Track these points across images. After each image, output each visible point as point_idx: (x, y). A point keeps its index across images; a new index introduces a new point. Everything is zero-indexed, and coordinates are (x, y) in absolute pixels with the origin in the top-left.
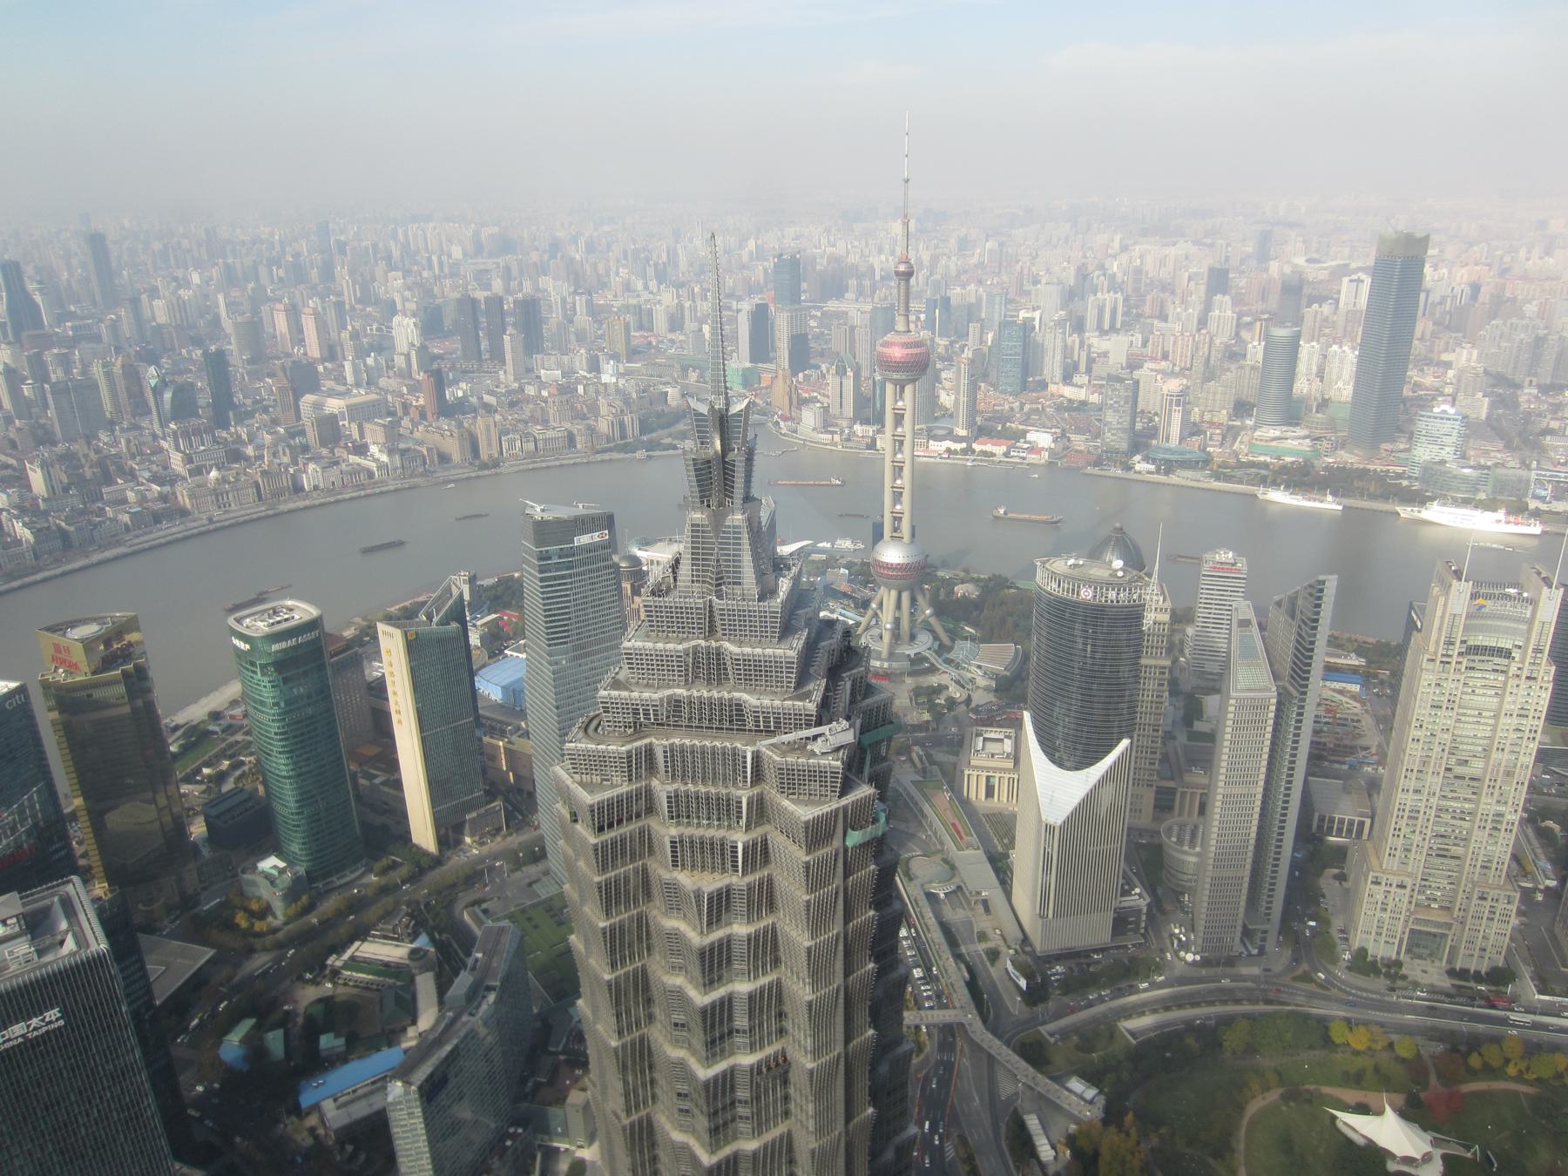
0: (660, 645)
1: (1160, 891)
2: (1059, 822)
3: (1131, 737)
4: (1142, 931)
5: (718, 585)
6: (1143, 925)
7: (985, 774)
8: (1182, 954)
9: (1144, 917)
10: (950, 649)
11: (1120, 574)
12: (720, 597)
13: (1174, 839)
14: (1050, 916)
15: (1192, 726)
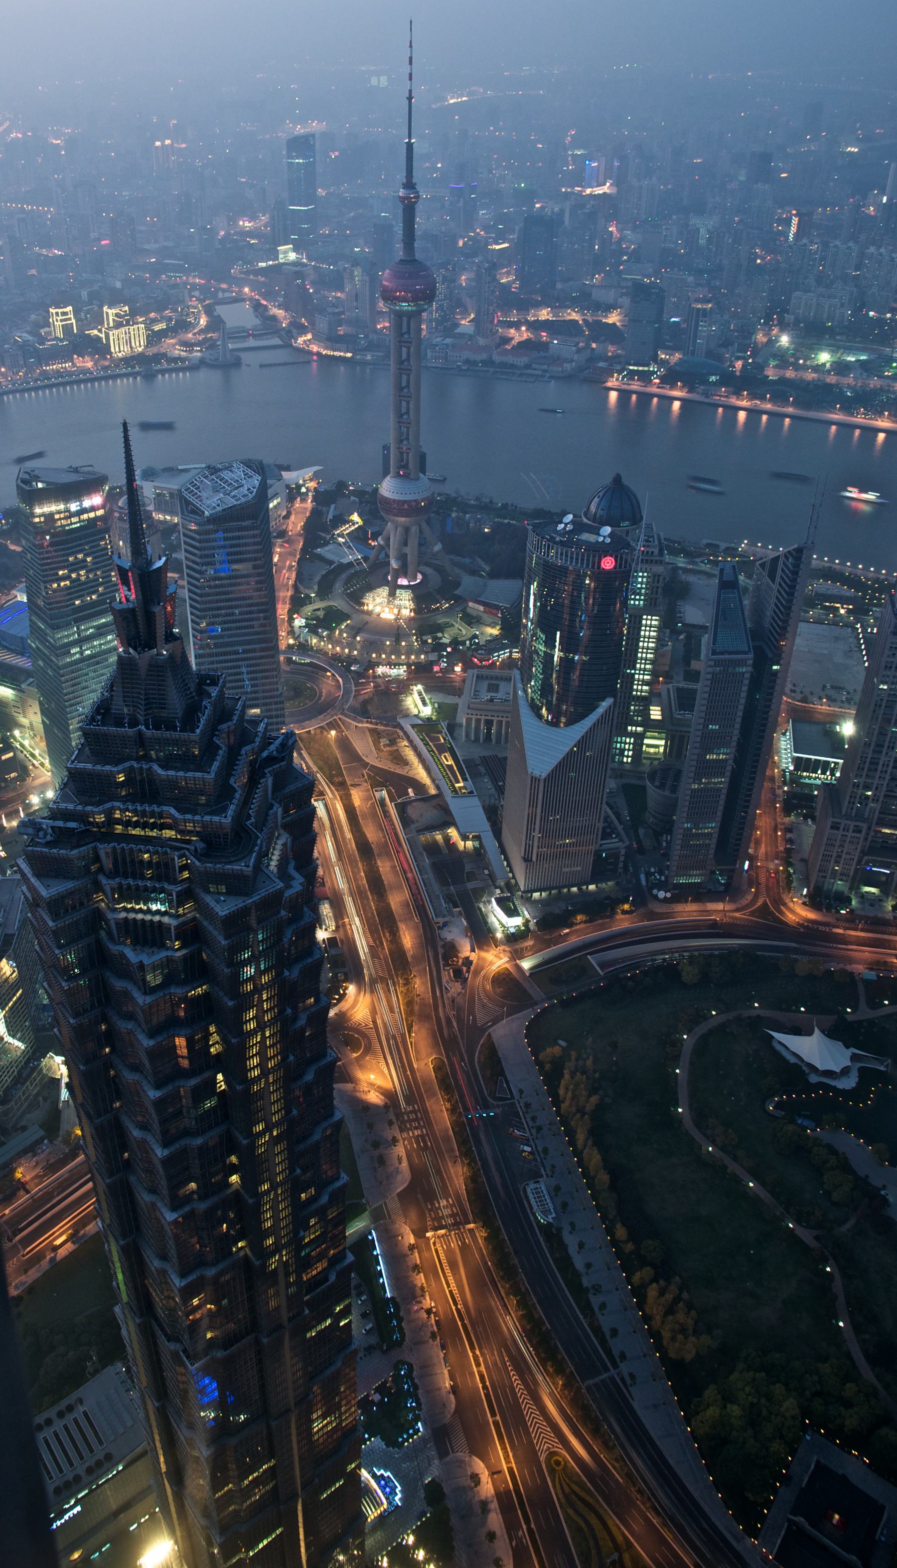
0: (98, 767)
1: (641, 831)
2: (544, 775)
3: (615, 697)
4: (620, 870)
5: (148, 704)
6: (621, 865)
7: (483, 718)
8: (655, 892)
9: (622, 859)
10: (457, 584)
11: (608, 540)
12: (148, 728)
13: (657, 783)
14: (534, 859)
15: (688, 663)
